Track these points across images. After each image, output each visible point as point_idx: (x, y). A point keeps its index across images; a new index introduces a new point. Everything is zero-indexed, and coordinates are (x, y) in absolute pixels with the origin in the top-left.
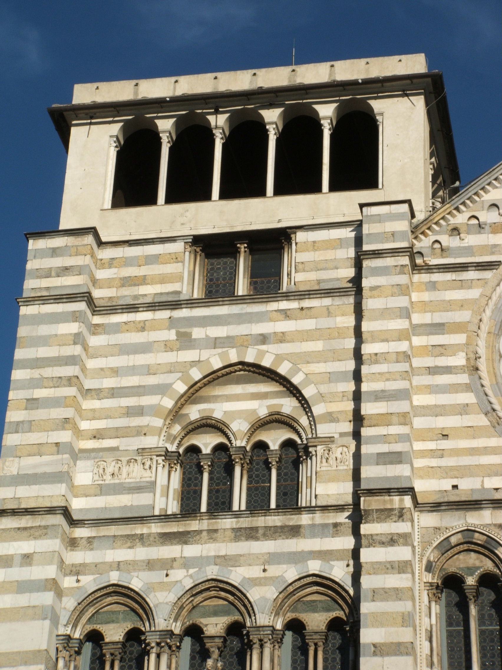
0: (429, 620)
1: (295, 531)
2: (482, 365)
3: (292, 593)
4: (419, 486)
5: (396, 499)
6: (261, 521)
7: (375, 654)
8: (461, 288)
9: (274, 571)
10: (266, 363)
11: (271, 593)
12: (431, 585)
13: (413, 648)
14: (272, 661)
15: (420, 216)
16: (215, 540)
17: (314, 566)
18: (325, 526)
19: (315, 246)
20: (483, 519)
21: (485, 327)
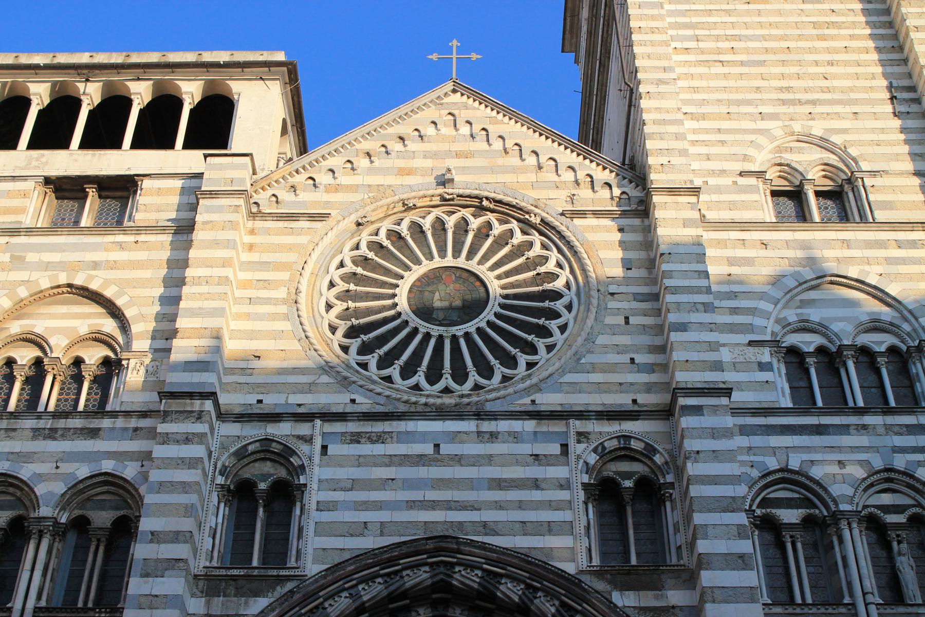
1: (94, 433)
2: (302, 299)
3: (82, 491)
4: (223, 399)
5: (198, 402)
6: (61, 423)
7: (151, 541)
8: (292, 234)
9: (66, 468)
10: (94, 286)
11: (59, 488)
12: (222, 486)
13: (192, 536)
14: (49, 552)
15: (261, 174)
16: (11, 438)
17: (108, 466)
18: (126, 429)
19: (159, 192)
20: (283, 430)
21: (309, 269)
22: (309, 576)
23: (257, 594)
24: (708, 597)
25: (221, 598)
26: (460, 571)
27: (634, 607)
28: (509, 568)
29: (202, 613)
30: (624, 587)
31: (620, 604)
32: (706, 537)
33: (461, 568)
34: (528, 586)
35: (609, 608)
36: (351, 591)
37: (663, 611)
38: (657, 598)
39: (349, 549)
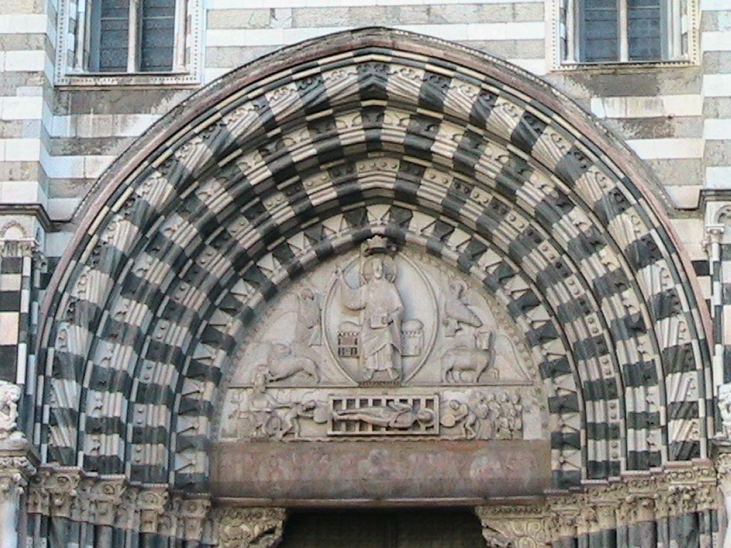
0: (75, 6)
22: (202, 85)
23: (136, 111)
24: (711, 110)
25: (92, 116)
26: (395, 72)
27: (620, 119)
28: (459, 68)
29: (68, 135)
30: (608, 92)
31: (600, 115)
32: (716, 27)
33: (398, 68)
34: (484, 92)
35: (587, 120)
36: (256, 102)
37: (656, 123)
38: (649, 105)
39: (252, 47)
